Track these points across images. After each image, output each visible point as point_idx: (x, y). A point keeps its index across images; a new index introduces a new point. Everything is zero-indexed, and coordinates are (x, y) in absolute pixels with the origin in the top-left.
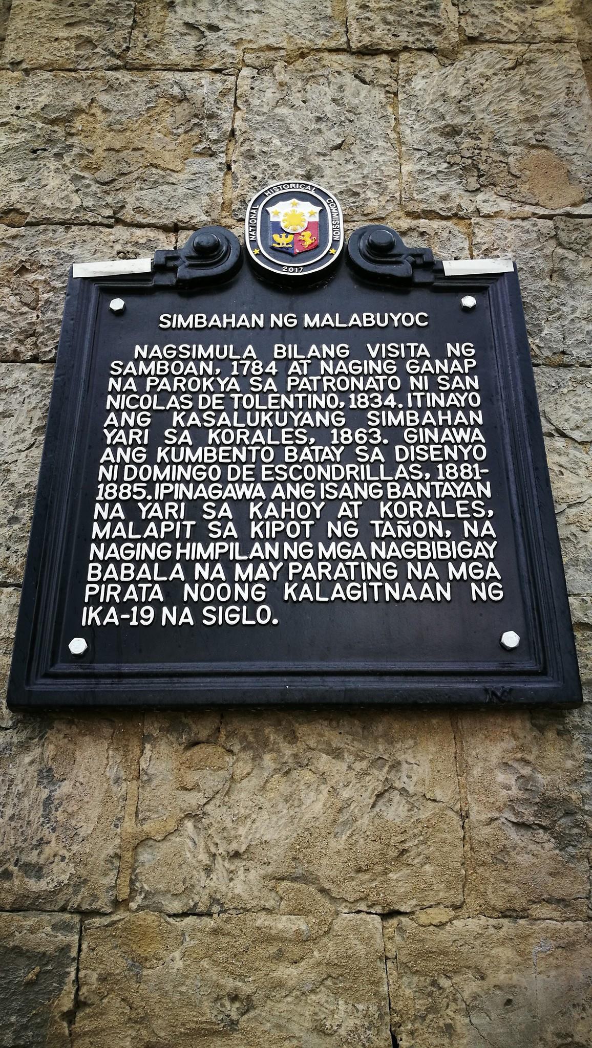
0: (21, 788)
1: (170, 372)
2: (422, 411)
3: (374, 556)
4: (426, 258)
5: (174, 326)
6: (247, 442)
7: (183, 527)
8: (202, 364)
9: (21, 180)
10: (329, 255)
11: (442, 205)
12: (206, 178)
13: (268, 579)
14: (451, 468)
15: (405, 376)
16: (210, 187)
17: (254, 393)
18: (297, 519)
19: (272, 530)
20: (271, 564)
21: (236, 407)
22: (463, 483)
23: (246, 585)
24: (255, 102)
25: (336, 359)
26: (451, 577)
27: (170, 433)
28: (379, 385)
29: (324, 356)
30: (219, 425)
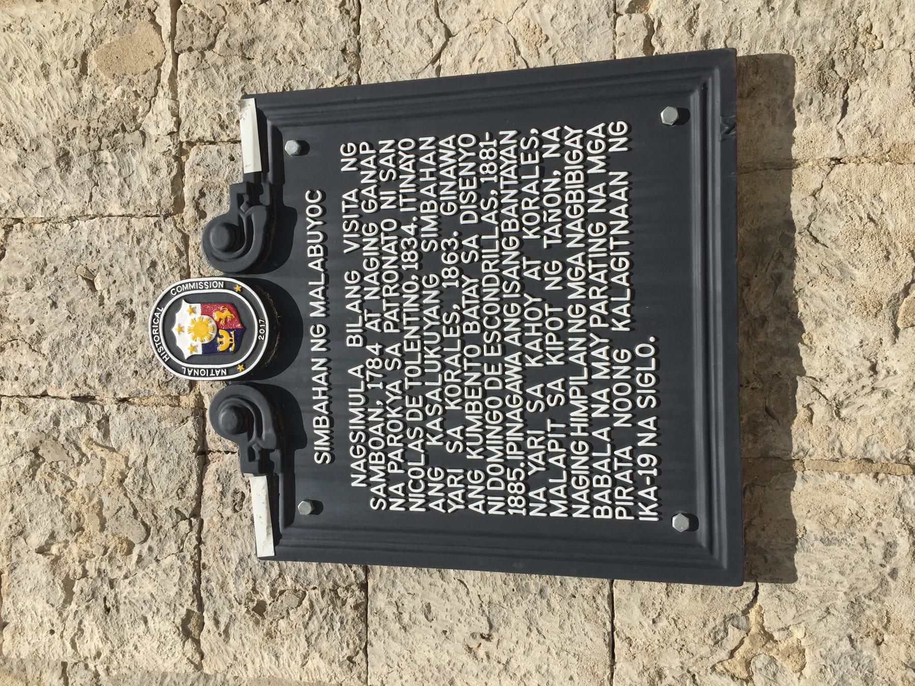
0: (814, 567)
1: (381, 451)
2: (420, 198)
3: (582, 245)
4: (243, 190)
5: (328, 449)
6: (459, 372)
7: (553, 430)
8: (370, 419)
9: (146, 622)
10: (242, 292)
11: (164, 172)
12: (138, 425)
13: (607, 347)
14: (484, 169)
15: (379, 215)
16: (149, 420)
17: (404, 366)
19: (555, 344)
20: (591, 345)
21: (419, 384)
22: (501, 158)
23: (614, 368)
24: (34, 375)
25: (362, 283)
26: (603, 171)
27: (451, 447)
28: (392, 241)
29: (358, 296)
30: (440, 400)
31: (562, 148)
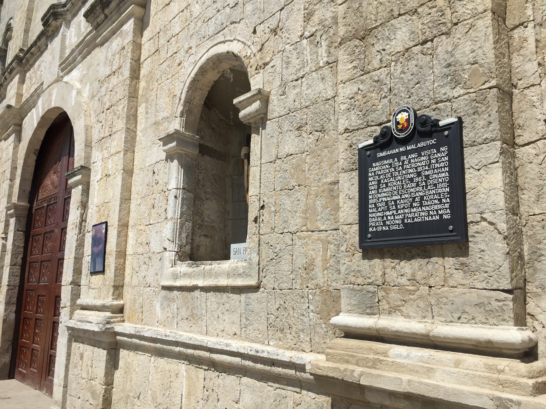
10: (411, 128)
11: (444, 97)
18: (407, 203)
19: (402, 207)
24: (395, 74)
25: (414, 158)
31: (444, 203)
